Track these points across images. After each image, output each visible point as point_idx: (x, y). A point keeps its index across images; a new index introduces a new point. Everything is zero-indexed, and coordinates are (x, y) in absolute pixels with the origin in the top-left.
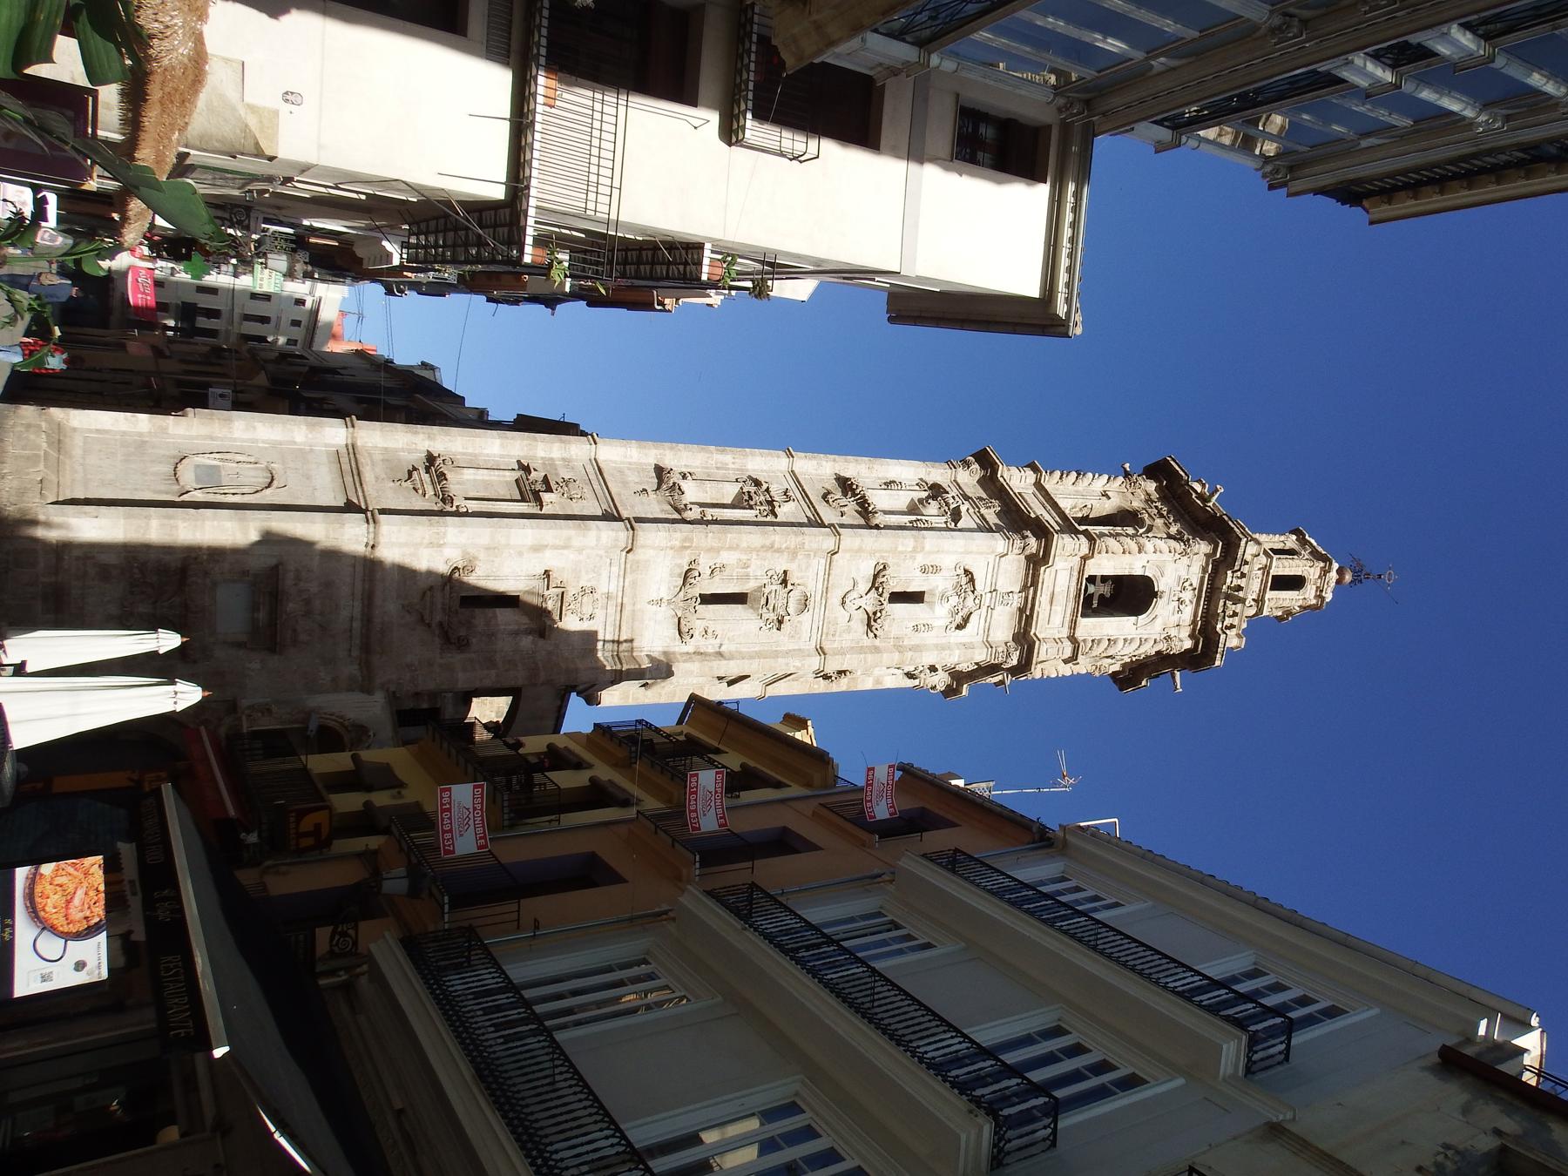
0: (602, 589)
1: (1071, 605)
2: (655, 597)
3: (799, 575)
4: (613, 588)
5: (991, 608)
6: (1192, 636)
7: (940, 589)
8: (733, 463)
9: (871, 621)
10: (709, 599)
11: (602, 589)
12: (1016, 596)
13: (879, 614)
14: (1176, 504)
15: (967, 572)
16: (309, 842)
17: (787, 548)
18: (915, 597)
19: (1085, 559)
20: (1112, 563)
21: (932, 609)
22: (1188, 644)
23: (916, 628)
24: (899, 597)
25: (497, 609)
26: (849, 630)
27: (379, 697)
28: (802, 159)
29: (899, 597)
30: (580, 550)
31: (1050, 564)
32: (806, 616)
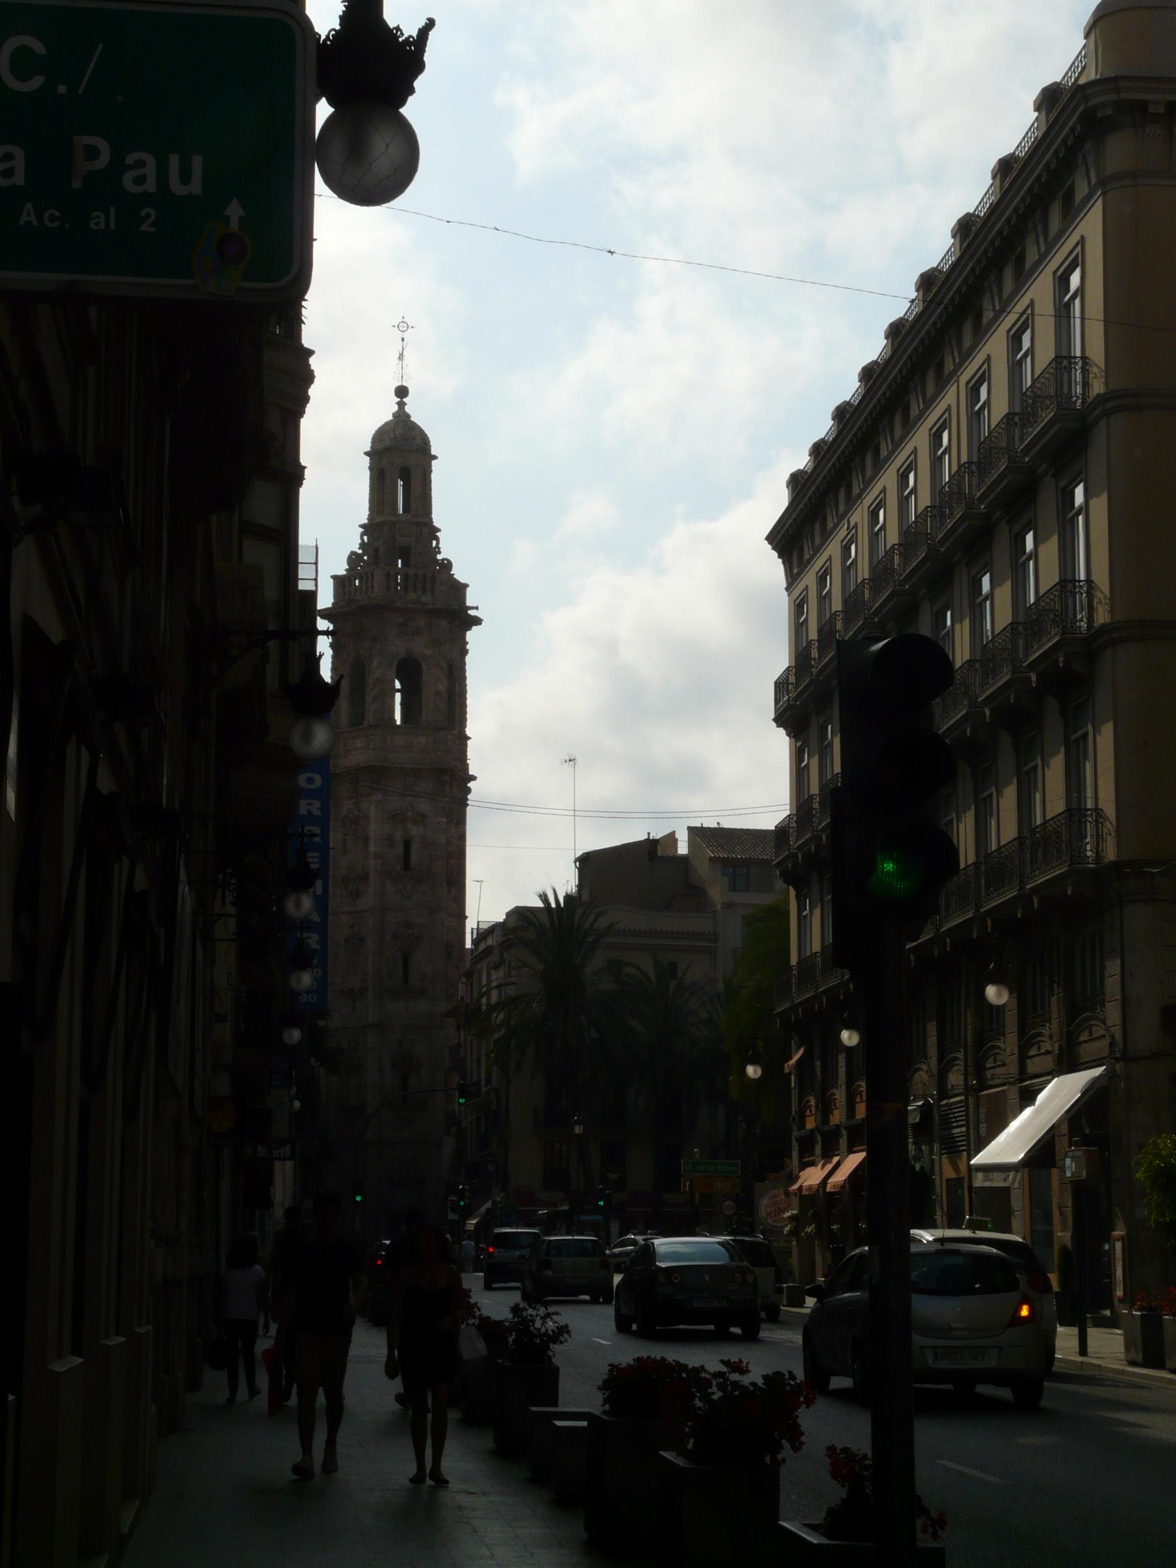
18: (407, 845)
24: (407, 865)
29: (407, 865)
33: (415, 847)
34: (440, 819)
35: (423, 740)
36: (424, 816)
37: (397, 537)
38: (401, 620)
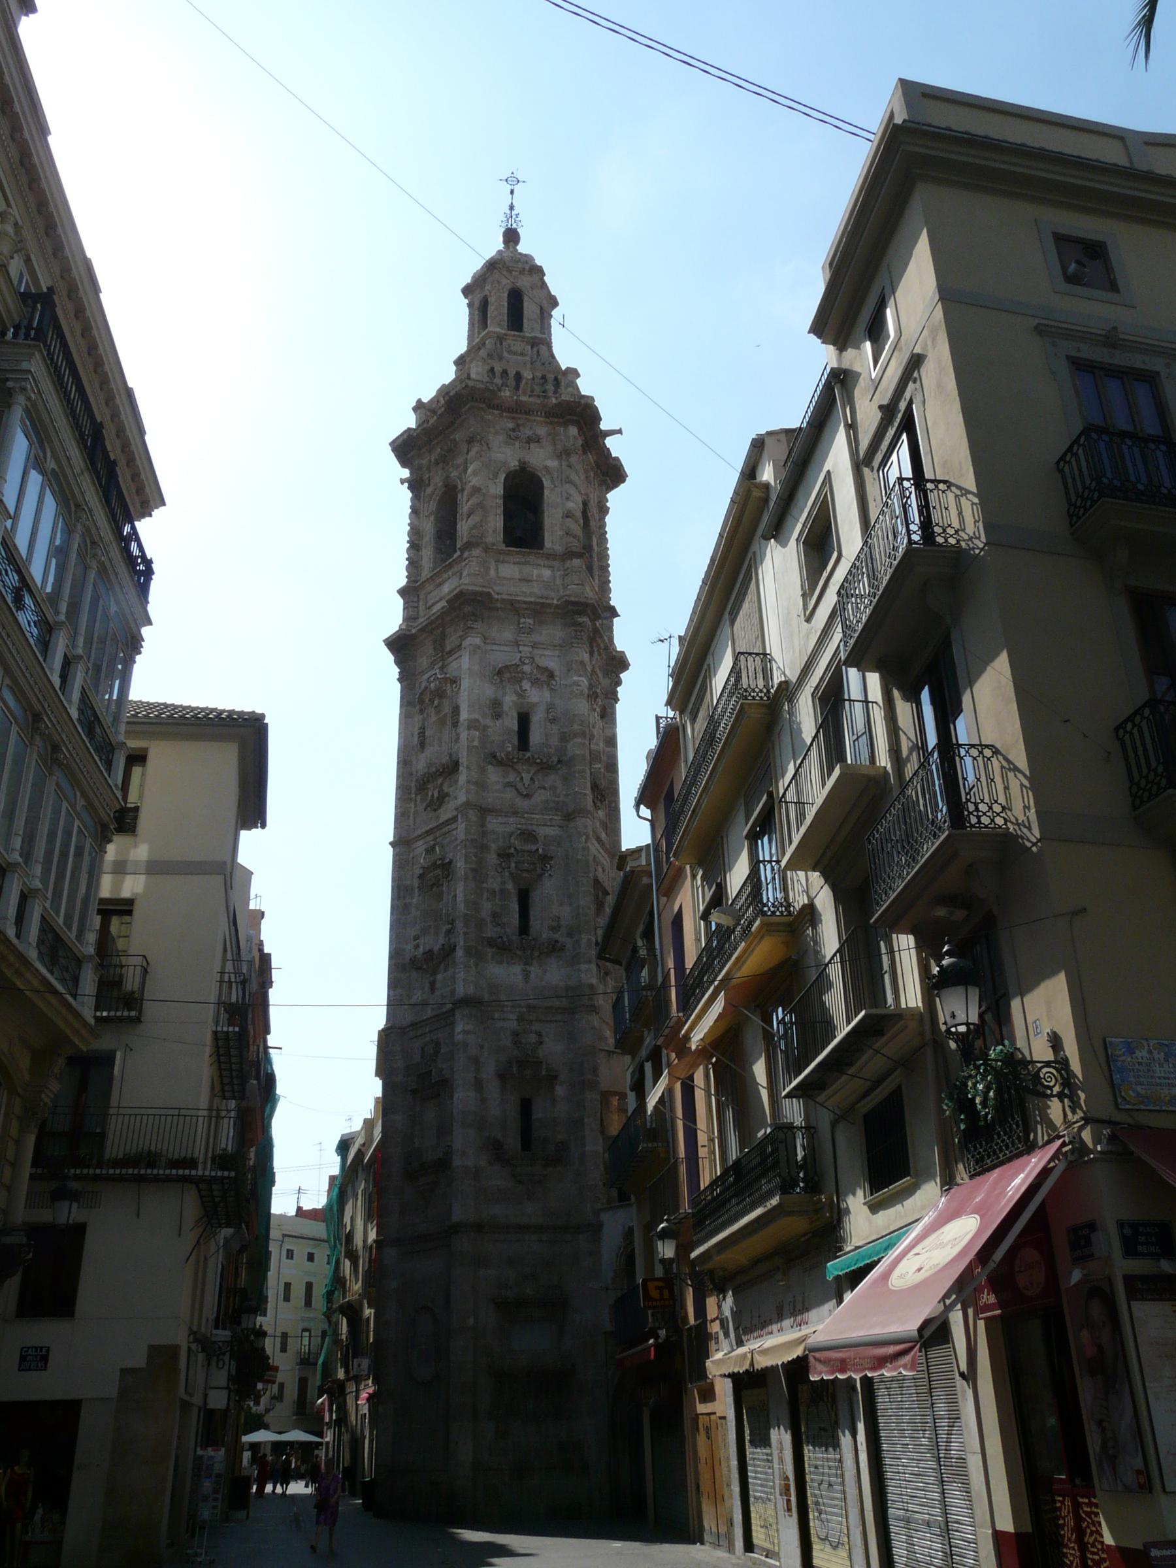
0: (514, 1025)
1: (532, 558)
3: (501, 840)
4: (513, 1017)
6: (566, 424)
7: (514, 698)
8: (404, 898)
9: (545, 767)
10: (524, 927)
11: (514, 1025)
12: (522, 620)
13: (538, 761)
14: (436, 441)
15: (500, 673)
16: (666, 1293)
17: (476, 856)
18: (524, 720)
19: (486, 550)
20: (491, 518)
21: (535, 705)
22: (573, 430)
25: (534, 1117)
26: (553, 788)
27: (606, 1217)
28: (145, 964)
30: (482, 1047)
31: (490, 590)
34: (575, 678)
35: (547, 573)
36: (551, 675)
37: (505, 354)
38: (511, 425)
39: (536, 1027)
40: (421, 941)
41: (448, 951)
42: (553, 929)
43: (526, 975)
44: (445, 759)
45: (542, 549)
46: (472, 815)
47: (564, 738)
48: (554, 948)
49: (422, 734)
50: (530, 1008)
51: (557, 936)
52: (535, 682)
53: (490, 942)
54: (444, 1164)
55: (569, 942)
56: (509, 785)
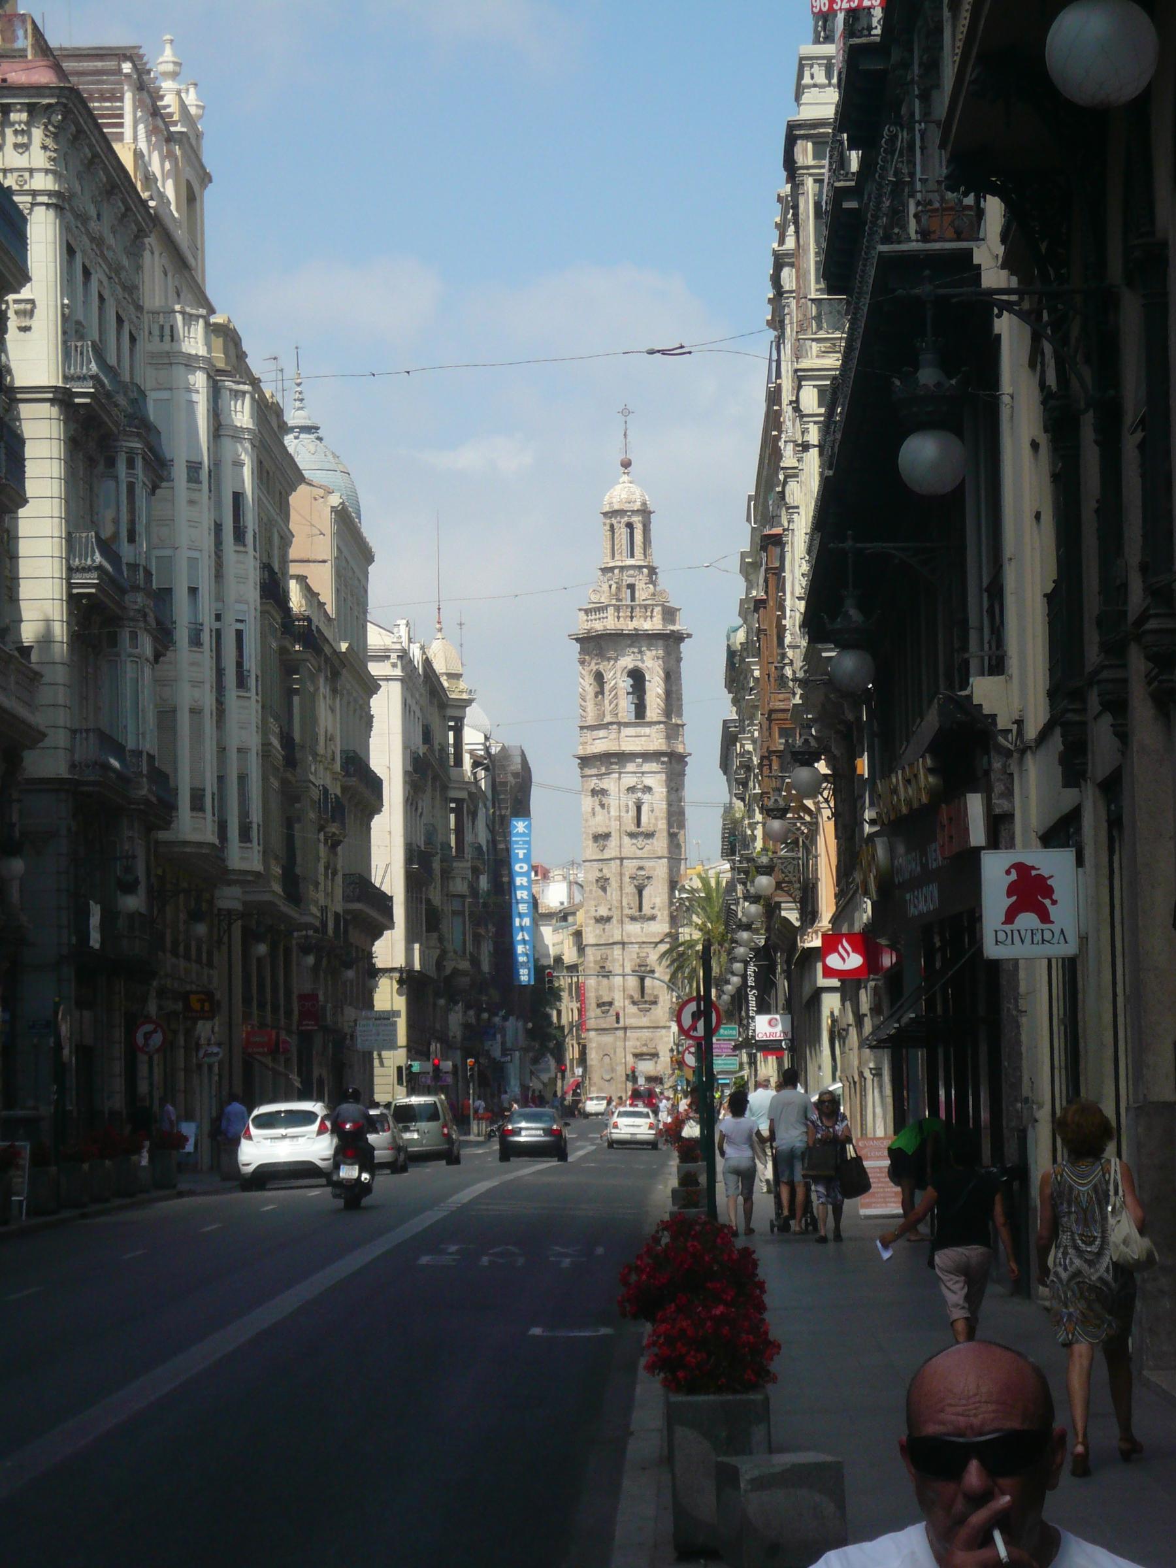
2: (639, 930)
5: (643, 773)
23: (652, 811)
24: (639, 824)
32: (648, 864)
33: (645, 809)
39: (646, 950)
40: (598, 908)
41: (608, 919)
42: (653, 908)
43: (642, 928)
44: (606, 831)
45: (644, 718)
46: (618, 862)
47: (656, 819)
48: (653, 918)
49: (593, 809)
50: (644, 943)
51: (654, 912)
52: (644, 792)
53: (628, 916)
54: (611, 1004)
55: (659, 914)
56: (634, 844)
